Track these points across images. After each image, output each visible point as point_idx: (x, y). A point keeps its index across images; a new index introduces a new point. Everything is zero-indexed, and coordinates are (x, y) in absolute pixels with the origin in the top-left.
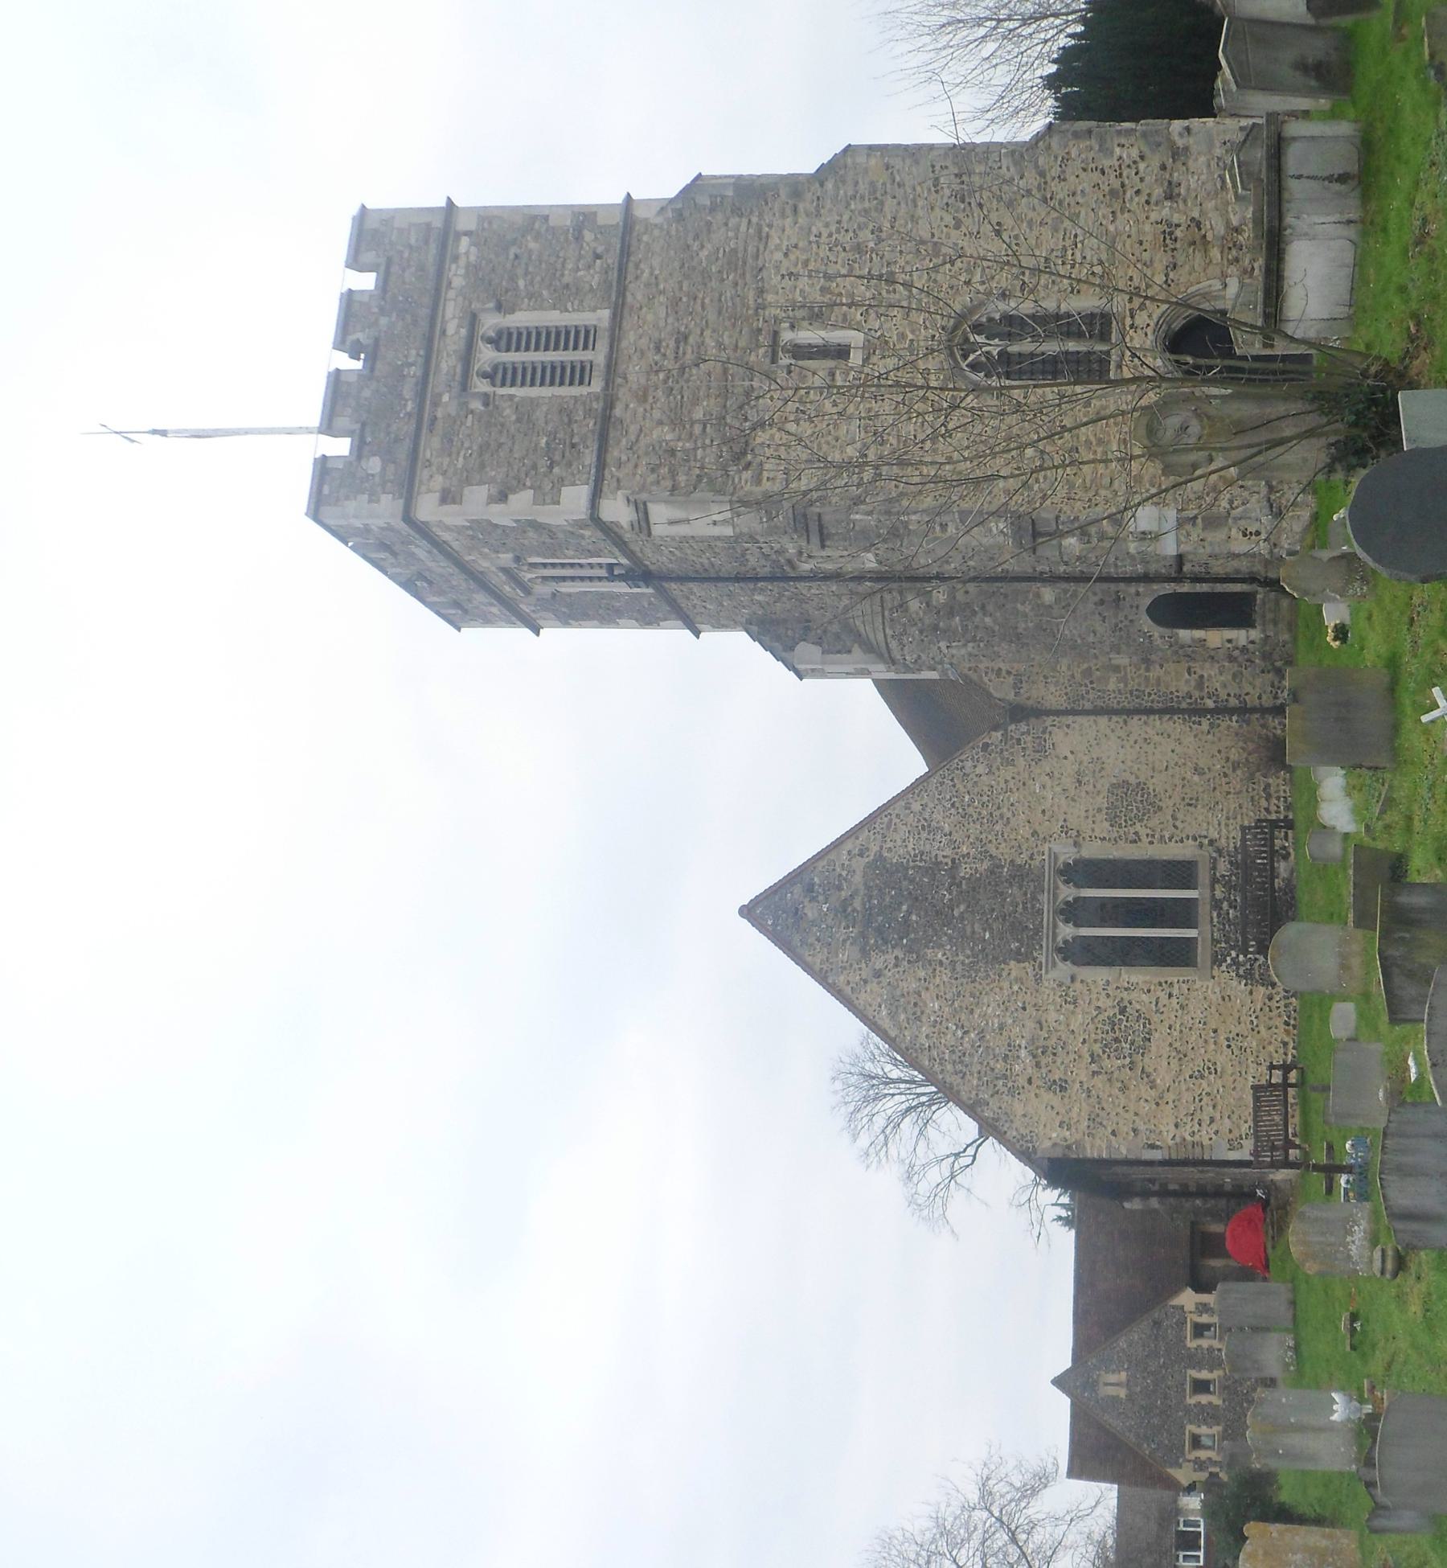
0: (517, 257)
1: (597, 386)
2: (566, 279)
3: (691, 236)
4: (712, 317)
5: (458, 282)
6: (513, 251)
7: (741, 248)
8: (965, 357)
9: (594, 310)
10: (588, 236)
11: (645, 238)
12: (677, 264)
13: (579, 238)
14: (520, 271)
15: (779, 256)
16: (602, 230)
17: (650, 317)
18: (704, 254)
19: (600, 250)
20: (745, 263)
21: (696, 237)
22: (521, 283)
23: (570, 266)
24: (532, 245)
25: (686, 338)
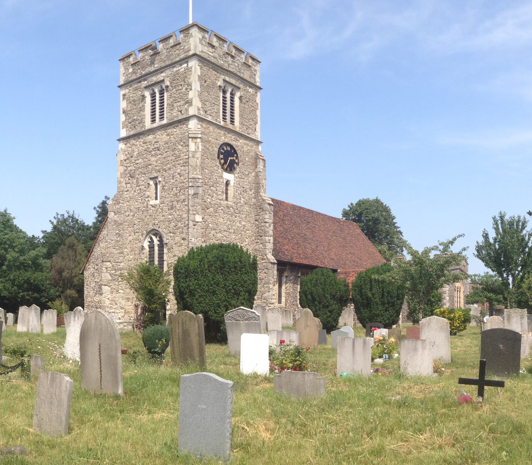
0: (181, 85)
1: (148, 124)
2: (175, 105)
3: (184, 141)
4: (163, 156)
5: (175, 69)
6: (182, 83)
7: (181, 158)
8: (154, 235)
9: (167, 118)
10: (186, 106)
11: (185, 126)
12: (177, 139)
13: (186, 103)
14: (178, 88)
15: (179, 171)
16: (187, 110)
17: (164, 136)
18: (180, 147)
19: (183, 112)
20: (177, 161)
21: (184, 143)
22: (174, 90)
23: (178, 104)
24: (184, 88)
25: (159, 150)
